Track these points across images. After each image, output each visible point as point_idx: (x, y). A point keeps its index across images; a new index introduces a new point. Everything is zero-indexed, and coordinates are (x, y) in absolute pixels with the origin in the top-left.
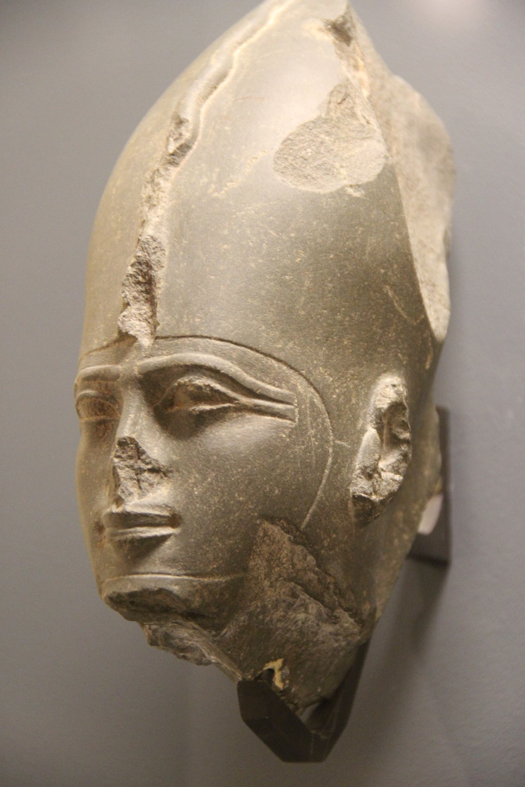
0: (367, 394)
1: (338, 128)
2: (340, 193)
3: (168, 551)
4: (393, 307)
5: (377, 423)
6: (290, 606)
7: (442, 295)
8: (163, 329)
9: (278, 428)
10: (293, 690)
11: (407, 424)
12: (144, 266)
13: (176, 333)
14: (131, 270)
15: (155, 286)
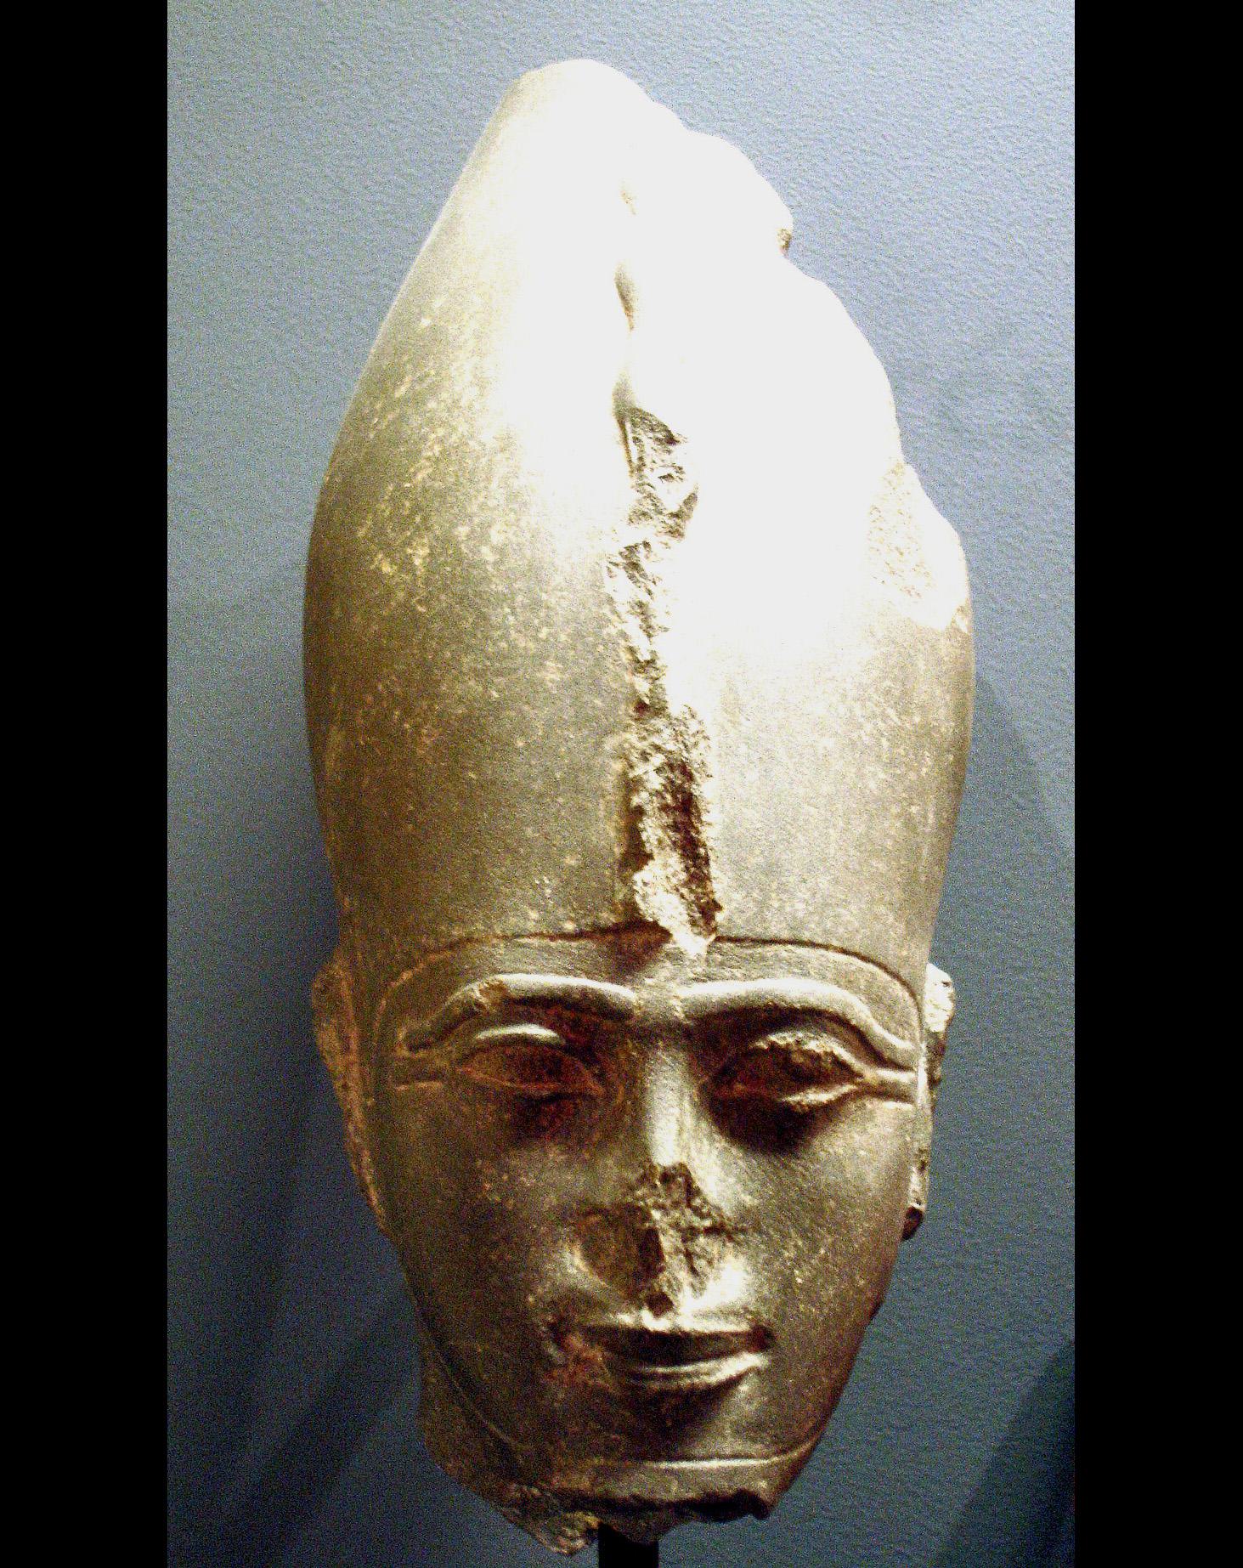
13: (759, 931)
15: (699, 817)
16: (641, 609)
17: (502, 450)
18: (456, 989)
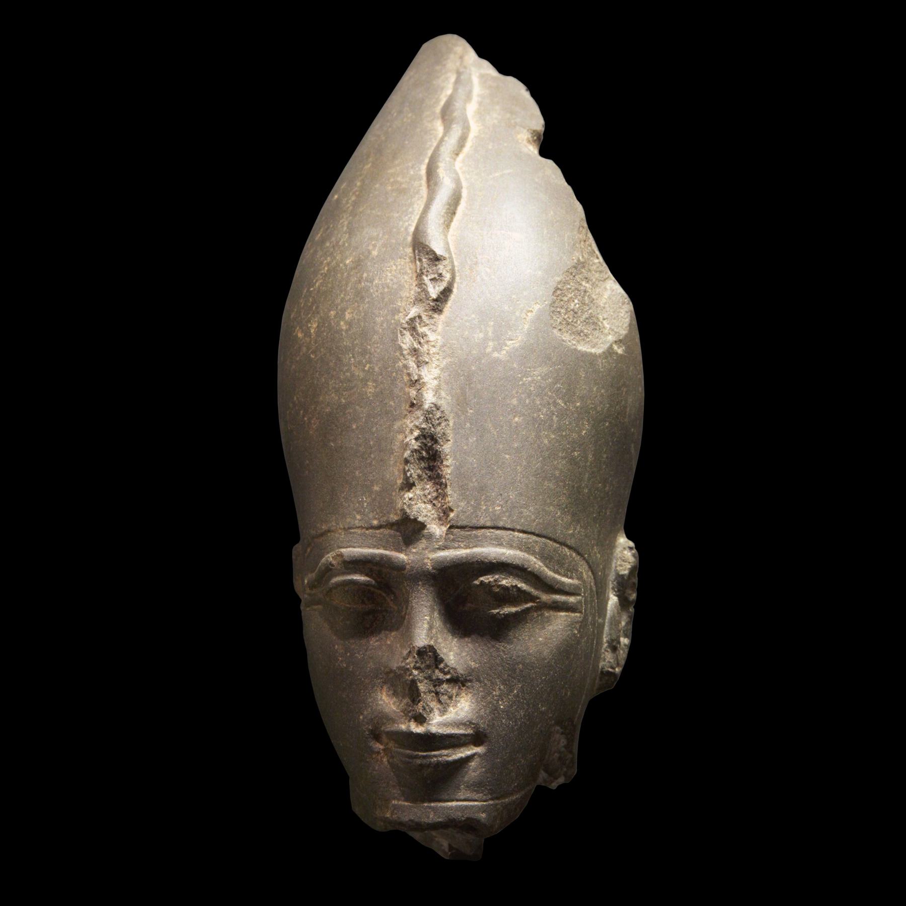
5: (619, 590)
12: (428, 439)
13: (474, 522)
16: (415, 352)
17: (355, 268)
18: (322, 557)
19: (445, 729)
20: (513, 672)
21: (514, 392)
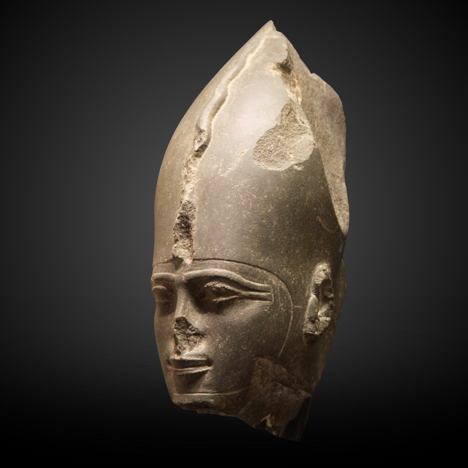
0: (310, 276)
1: (287, 130)
2: (291, 169)
3: (206, 380)
4: (322, 227)
5: (316, 292)
6: (274, 391)
7: (345, 205)
8: (197, 254)
9: (263, 307)
10: (277, 425)
11: (332, 289)
13: (205, 257)
14: (177, 221)
19: (190, 357)
20: (226, 330)
21: (229, 192)
